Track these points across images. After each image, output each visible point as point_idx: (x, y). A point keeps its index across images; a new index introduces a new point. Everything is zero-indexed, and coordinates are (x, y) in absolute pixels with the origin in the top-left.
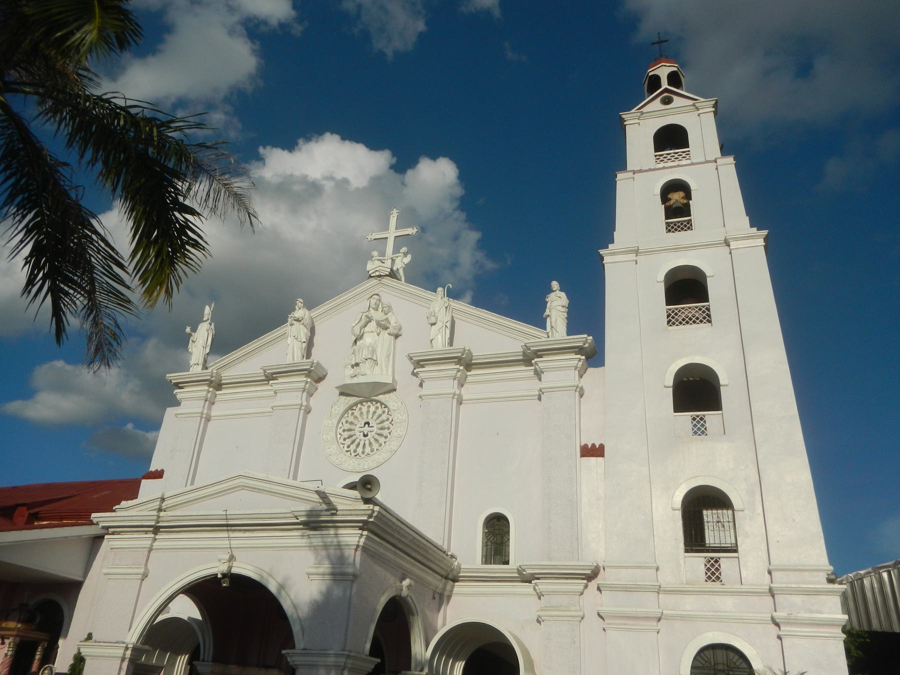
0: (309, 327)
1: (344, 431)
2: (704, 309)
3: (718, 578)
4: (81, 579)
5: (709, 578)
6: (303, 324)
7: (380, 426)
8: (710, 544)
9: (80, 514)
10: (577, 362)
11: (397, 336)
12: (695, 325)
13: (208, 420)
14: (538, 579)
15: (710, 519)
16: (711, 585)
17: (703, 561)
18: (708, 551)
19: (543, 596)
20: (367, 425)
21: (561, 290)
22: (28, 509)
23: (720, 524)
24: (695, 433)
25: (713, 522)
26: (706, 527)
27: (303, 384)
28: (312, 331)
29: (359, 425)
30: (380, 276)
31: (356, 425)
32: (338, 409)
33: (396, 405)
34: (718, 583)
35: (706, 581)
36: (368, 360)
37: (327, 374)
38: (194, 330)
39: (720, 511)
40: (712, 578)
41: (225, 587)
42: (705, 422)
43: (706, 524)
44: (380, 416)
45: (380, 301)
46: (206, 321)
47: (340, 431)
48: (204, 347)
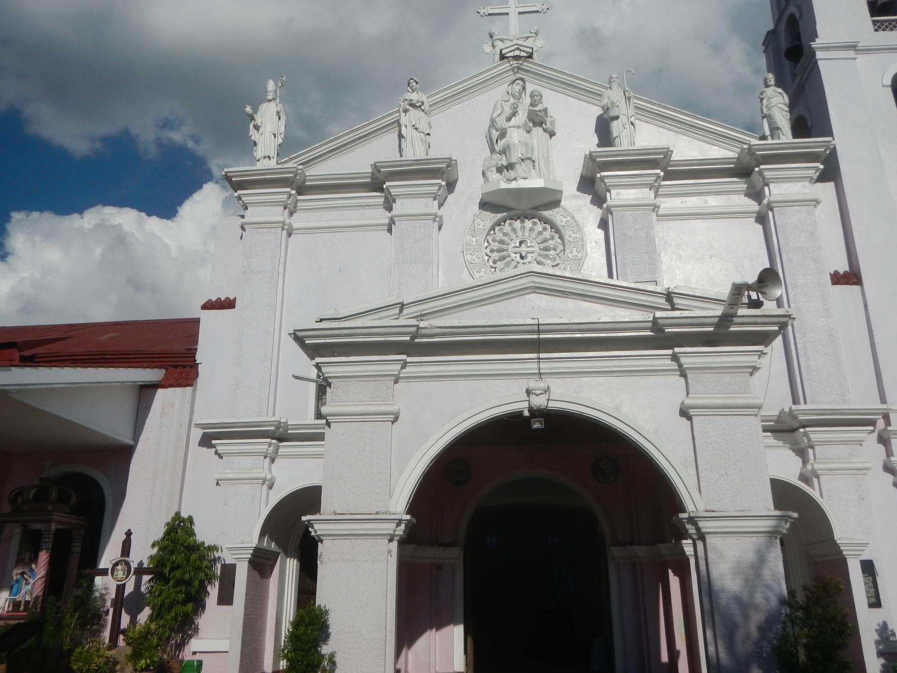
1: (492, 251)
4: (131, 442)
6: (423, 111)
7: (542, 246)
9: (107, 357)
10: (813, 172)
11: (552, 134)
13: (289, 235)
14: (808, 426)
19: (812, 447)
20: (523, 245)
21: (778, 85)
22: (19, 351)
27: (437, 188)
29: (513, 245)
30: (517, 58)
31: (508, 244)
32: (482, 223)
33: (564, 220)
36: (525, 162)
37: (458, 179)
38: (255, 110)
41: (537, 430)
45: (524, 88)
46: (270, 101)
47: (488, 251)
48: (275, 135)
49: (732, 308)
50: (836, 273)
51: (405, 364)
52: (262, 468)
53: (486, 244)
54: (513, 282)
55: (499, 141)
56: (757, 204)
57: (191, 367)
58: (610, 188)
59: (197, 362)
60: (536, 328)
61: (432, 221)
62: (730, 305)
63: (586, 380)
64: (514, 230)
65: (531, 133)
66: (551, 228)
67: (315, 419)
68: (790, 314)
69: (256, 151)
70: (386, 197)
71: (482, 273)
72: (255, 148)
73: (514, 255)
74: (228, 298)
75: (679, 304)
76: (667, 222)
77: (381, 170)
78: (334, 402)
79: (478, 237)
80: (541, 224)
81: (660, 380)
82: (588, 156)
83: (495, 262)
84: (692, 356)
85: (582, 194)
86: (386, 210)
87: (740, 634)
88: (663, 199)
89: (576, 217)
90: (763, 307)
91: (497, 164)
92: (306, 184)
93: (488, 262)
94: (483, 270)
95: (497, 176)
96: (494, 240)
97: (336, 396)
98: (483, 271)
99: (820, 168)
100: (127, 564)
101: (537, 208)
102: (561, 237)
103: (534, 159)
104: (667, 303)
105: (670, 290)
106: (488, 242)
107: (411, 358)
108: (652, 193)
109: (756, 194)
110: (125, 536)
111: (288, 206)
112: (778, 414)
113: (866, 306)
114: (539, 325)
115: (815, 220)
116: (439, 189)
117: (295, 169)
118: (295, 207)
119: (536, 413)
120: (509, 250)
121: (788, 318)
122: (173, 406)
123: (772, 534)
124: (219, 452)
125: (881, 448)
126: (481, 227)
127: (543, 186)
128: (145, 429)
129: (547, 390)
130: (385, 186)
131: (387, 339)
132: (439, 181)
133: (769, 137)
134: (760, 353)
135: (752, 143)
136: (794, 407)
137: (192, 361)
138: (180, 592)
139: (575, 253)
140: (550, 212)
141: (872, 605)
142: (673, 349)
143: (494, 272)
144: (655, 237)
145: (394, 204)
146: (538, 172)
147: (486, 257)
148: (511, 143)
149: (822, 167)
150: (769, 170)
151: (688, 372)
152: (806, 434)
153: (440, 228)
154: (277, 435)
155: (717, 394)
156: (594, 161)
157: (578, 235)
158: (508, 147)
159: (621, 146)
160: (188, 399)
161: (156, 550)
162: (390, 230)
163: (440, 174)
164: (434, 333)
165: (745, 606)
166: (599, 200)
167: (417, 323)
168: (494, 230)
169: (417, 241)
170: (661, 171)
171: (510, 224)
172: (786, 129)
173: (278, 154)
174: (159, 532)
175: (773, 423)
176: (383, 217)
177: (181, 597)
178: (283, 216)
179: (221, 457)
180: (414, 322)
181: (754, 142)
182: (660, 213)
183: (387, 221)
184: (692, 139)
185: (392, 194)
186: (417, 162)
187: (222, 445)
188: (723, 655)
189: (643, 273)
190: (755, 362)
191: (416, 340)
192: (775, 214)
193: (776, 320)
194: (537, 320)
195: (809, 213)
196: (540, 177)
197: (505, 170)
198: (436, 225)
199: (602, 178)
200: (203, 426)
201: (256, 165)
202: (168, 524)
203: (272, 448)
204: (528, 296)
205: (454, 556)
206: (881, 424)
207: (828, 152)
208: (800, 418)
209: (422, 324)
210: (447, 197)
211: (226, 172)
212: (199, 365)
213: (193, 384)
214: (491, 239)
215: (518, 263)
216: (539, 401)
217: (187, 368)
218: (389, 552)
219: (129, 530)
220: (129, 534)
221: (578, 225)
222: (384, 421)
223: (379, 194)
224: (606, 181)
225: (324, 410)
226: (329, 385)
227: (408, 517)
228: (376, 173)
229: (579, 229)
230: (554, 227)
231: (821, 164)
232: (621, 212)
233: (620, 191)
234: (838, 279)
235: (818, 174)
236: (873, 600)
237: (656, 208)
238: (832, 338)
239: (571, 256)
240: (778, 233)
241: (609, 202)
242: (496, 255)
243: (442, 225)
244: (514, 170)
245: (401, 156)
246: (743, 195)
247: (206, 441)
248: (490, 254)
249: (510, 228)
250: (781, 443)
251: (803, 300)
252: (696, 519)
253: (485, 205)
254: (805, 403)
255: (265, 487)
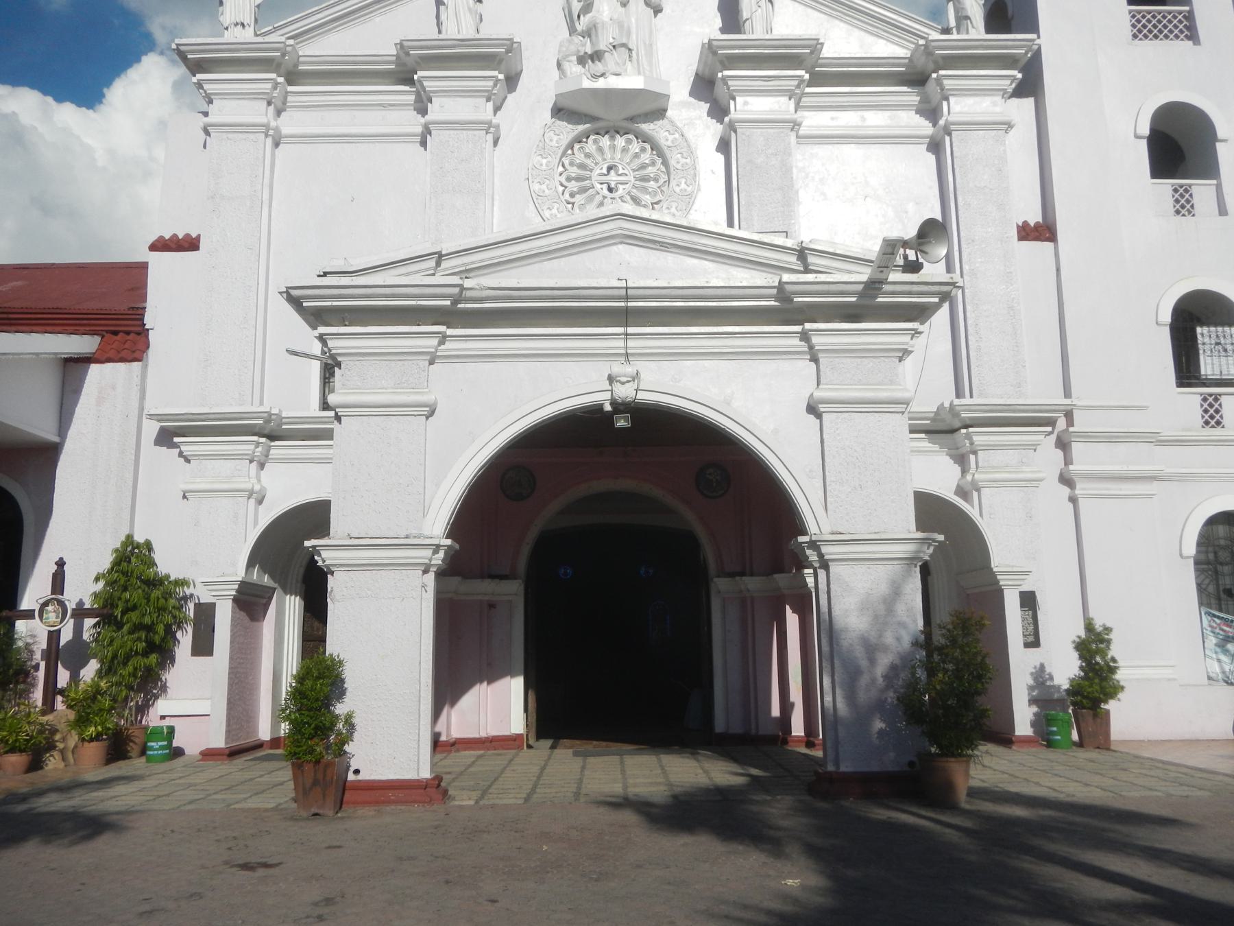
1: (569, 179)
2: (1180, 17)
3: (1218, 423)
4: (56, 439)
5: (1207, 423)
7: (638, 174)
8: (1206, 375)
9: (11, 316)
10: (1008, 82)
12: (1166, 42)
14: (971, 426)
15: (1207, 340)
16: (1208, 431)
17: (1199, 399)
18: (1204, 385)
19: (975, 453)
20: (612, 172)
23: (1220, 347)
24: (1178, 212)
25: (1211, 344)
26: (1201, 352)
27: (491, 83)
29: (598, 171)
31: (591, 170)
32: (555, 138)
34: (1219, 428)
35: (1203, 427)
37: (522, 71)
39: (1220, 329)
40: (1210, 423)
41: (622, 429)
42: (1191, 195)
43: (1200, 346)
44: (636, 156)
47: (563, 179)
49: (882, 272)
50: (1025, 224)
51: (444, 339)
52: (246, 477)
53: (561, 169)
54: (594, 227)
55: (582, 17)
56: (931, 125)
57: (139, 334)
58: (735, 94)
59: (147, 327)
60: (623, 292)
61: (484, 132)
62: (879, 267)
63: (688, 364)
64: (600, 150)
65: (627, 6)
66: (652, 149)
67: (320, 410)
68: (955, 281)
69: (222, 14)
70: (418, 94)
71: (554, 211)
72: (221, 9)
73: (599, 186)
74: (188, 236)
75: (814, 264)
76: (814, 146)
77: (411, 52)
78: (345, 389)
79: (550, 159)
80: (638, 142)
81: (784, 365)
82: (707, 46)
83: (572, 195)
84: (827, 334)
85: (696, 101)
86: (418, 113)
87: (864, 681)
88: (806, 114)
89: (686, 135)
90: (922, 272)
91: (578, 51)
92: (300, 68)
93: (563, 194)
94: (556, 206)
95: (578, 69)
96: (572, 164)
97: (348, 381)
98: (556, 207)
99: (1017, 77)
100: (62, 604)
101: (632, 119)
102: (665, 163)
103: (630, 47)
104: (799, 262)
105: (804, 245)
106: (563, 166)
107: (451, 330)
108: (792, 104)
109: (931, 112)
110: (55, 567)
111: (273, 101)
112: (935, 410)
113: (1058, 270)
114: (627, 288)
115: (1005, 151)
116: (495, 85)
117: (282, 45)
118: (284, 102)
119: (620, 407)
120: (593, 179)
121: (952, 287)
122: (114, 388)
123: (911, 560)
124: (185, 454)
125: (1060, 453)
126: (554, 143)
127: (641, 86)
128: (74, 420)
129: (636, 377)
130: (416, 77)
131: (419, 303)
132: (495, 73)
133: (954, 30)
134: (913, 332)
135: (930, 38)
136: (957, 402)
137: (139, 326)
138: (139, 639)
139: (683, 186)
140: (652, 126)
141: (1027, 645)
142: (803, 324)
143: (571, 210)
144: (792, 167)
145: (429, 104)
146: (636, 66)
147: (560, 186)
148: (598, 21)
149: (1020, 76)
150: (950, 78)
151: (820, 355)
152: (969, 437)
153: (496, 143)
154: (266, 432)
155: (856, 385)
156: (715, 53)
157: (688, 161)
158: (595, 26)
159: (753, 33)
160: (137, 380)
161: (101, 584)
162: (424, 144)
163: (496, 63)
164: (484, 296)
165: (872, 649)
166: (719, 111)
167: (460, 282)
168: (572, 148)
169: (463, 160)
170: (806, 73)
171: (595, 141)
172: (978, 18)
173: (256, 20)
174: (105, 562)
175: (928, 422)
176: (414, 123)
177: (141, 646)
178: (266, 115)
179: (188, 461)
180: (455, 280)
181: (934, 35)
182: (801, 132)
183: (419, 130)
184: (850, 27)
185: (427, 89)
186: (463, 42)
187: (190, 445)
188: (841, 705)
189: (774, 218)
190: (907, 344)
191: (459, 306)
192: (953, 140)
193: (936, 288)
194: (625, 281)
195: (998, 140)
196: (639, 73)
197: (590, 61)
198: (490, 138)
199: (724, 79)
200: (159, 417)
201: (226, 36)
202: (116, 550)
203: (260, 449)
204: (614, 248)
205: (512, 591)
206: (1061, 424)
207: (1029, 55)
208: (963, 415)
209: (468, 283)
210: (506, 97)
211: (177, 45)
212: (150, 331)
213: (143, 357)
214: (567, 161)
215: (604, 197)
216: (625, 392)
217: (132, 335)
218: (424, 586)
219: (61, 559)
220: (61, 564)
221: (689, 146)
222: (415, 416)
223: (407, 88)
224: (730, 83)
225: (332, 399)
226: (339, 365)
227: (449, 542)
228: (402, 55)
229: (691, 152)
230: (656, 147)
231: (1019, 72)
232: (748, 130)
233: (749, 99)
234: (1027, 233)
235: (1014, 85)
236: (1031, 639)
237: (795, 125)
238: (1012, 312)
239: (677, 189)
240: (955, 166)
241: (734, 115)
242: (574, 186)
243: (498, 139)
244: (603, 61)
245: (440, 32)
246: (914, 112)
247: (166, 438)
248: (565, 183)
249: (594, 147)
250: (937, 447)
251: (979, 260)
252: (818, 543)
253: (559, 112)
254: (971, 396)
255: (252, 501)
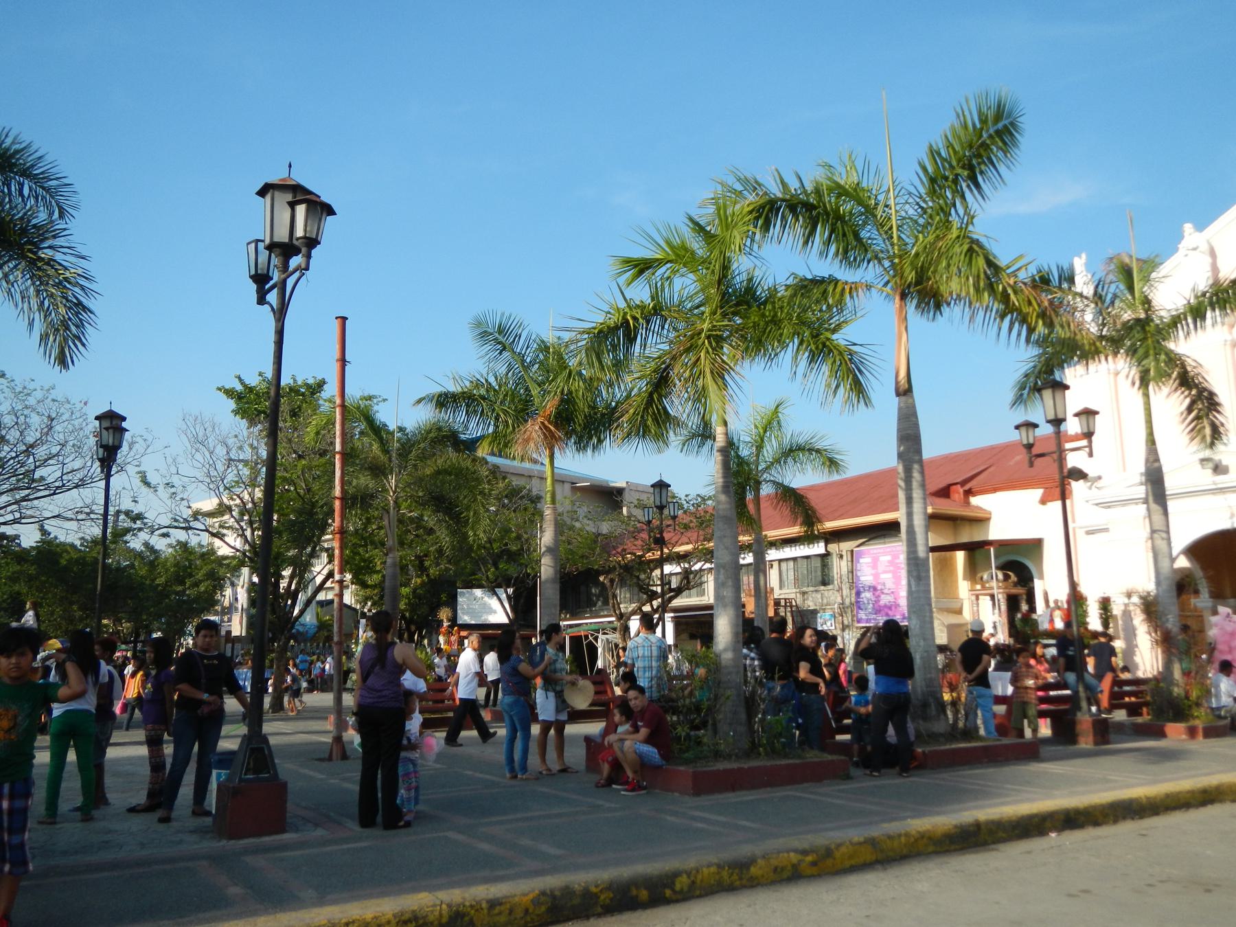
0: (1208, 252)
28: (1213, 254)
